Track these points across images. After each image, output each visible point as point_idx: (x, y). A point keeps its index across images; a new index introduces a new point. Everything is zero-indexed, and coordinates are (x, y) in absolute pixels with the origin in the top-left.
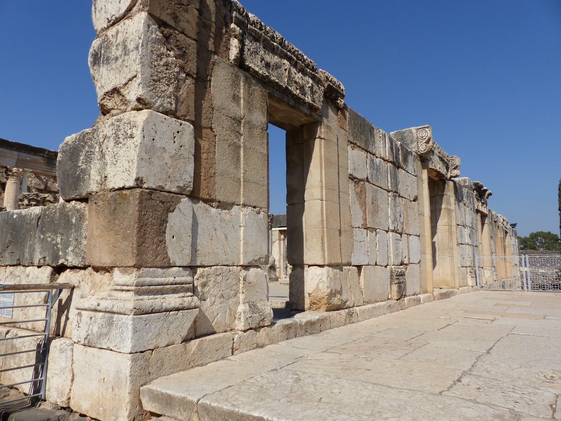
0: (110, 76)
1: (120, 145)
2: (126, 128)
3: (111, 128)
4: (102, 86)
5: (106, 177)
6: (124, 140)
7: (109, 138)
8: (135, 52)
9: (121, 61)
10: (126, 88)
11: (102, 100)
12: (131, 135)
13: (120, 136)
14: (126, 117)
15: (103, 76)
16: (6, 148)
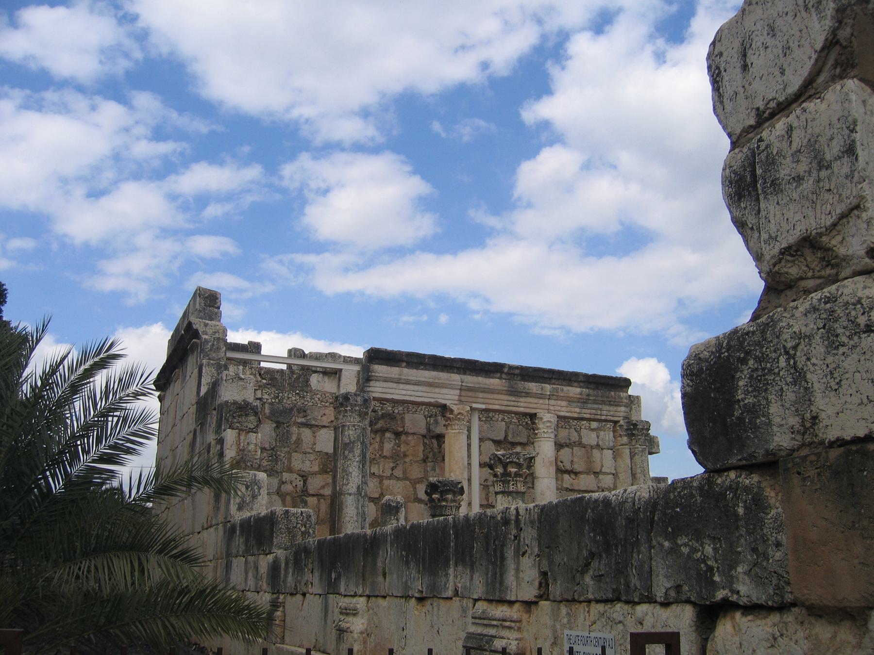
0: (790, 215)
1: (842, 350)
2: (853, 313)
3: (812, 317)
4: (770, 237)
5: (814, 418)
6: (850, 338)
7: (810, 337)
8: (846, 159)
9: (811, 182)
10: (834, 233)
11: (774, 265)
12: (867, 325)
13: (840, 331)
14: (846, 291)
15: (771, 217)
16: (442, 371)
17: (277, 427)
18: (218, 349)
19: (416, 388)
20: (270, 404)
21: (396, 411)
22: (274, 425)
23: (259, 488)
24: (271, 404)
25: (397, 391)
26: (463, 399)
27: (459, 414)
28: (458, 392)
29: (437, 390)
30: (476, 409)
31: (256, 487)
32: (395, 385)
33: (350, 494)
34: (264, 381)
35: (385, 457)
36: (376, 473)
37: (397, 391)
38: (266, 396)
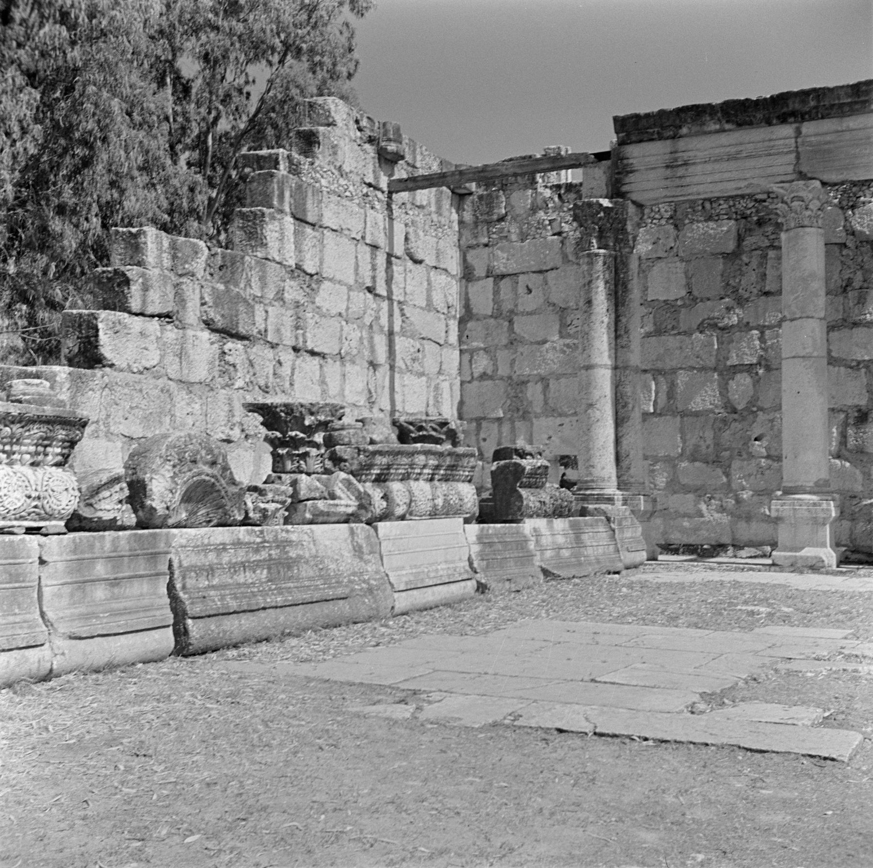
28: (793, 156)
35: (767, 294)
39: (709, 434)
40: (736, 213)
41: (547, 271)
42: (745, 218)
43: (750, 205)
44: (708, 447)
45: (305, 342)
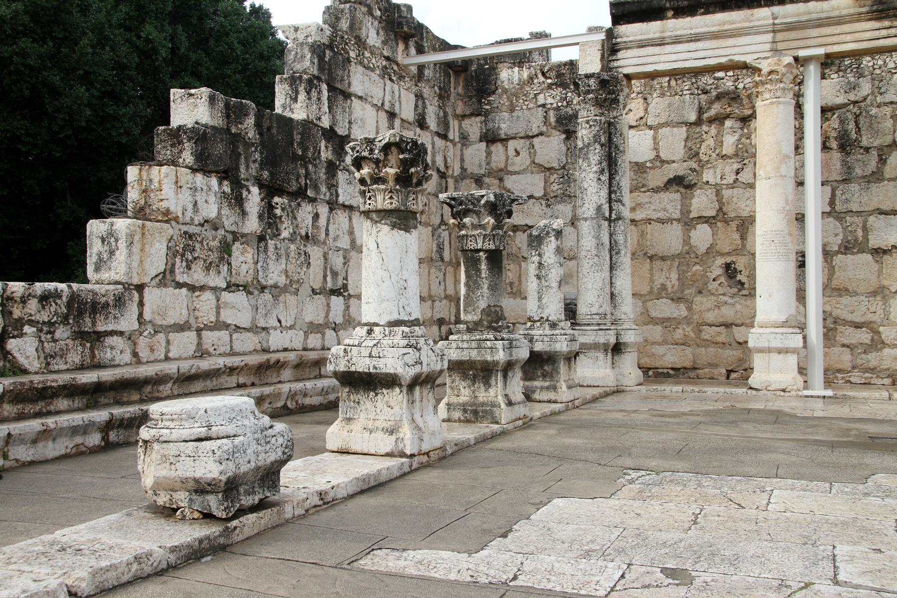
17: (568, 138)
18: (303, 57)
19: (693, 46)
20: (554, 109)
21: (741, 86)
22: (564, 136)
23: (117, 240)
24: (557, 109)
25: (662, 58)
26: (780, 46)
27: (770, 73)
28: (769, 37)
29: (730, 42)
30: (807, 60)
31: (113, 239)
32: (657, 50)
33: (586, 219)
34: (549, 81)
36: (712, 181)
37: (662, 58)
38: (550, 100)
39: (674, 276)
40: (698, 89)
41: (533, 137)
42: (706, 93)
43: (711, 82)
44: (673, 287)
45: (337, 196)
